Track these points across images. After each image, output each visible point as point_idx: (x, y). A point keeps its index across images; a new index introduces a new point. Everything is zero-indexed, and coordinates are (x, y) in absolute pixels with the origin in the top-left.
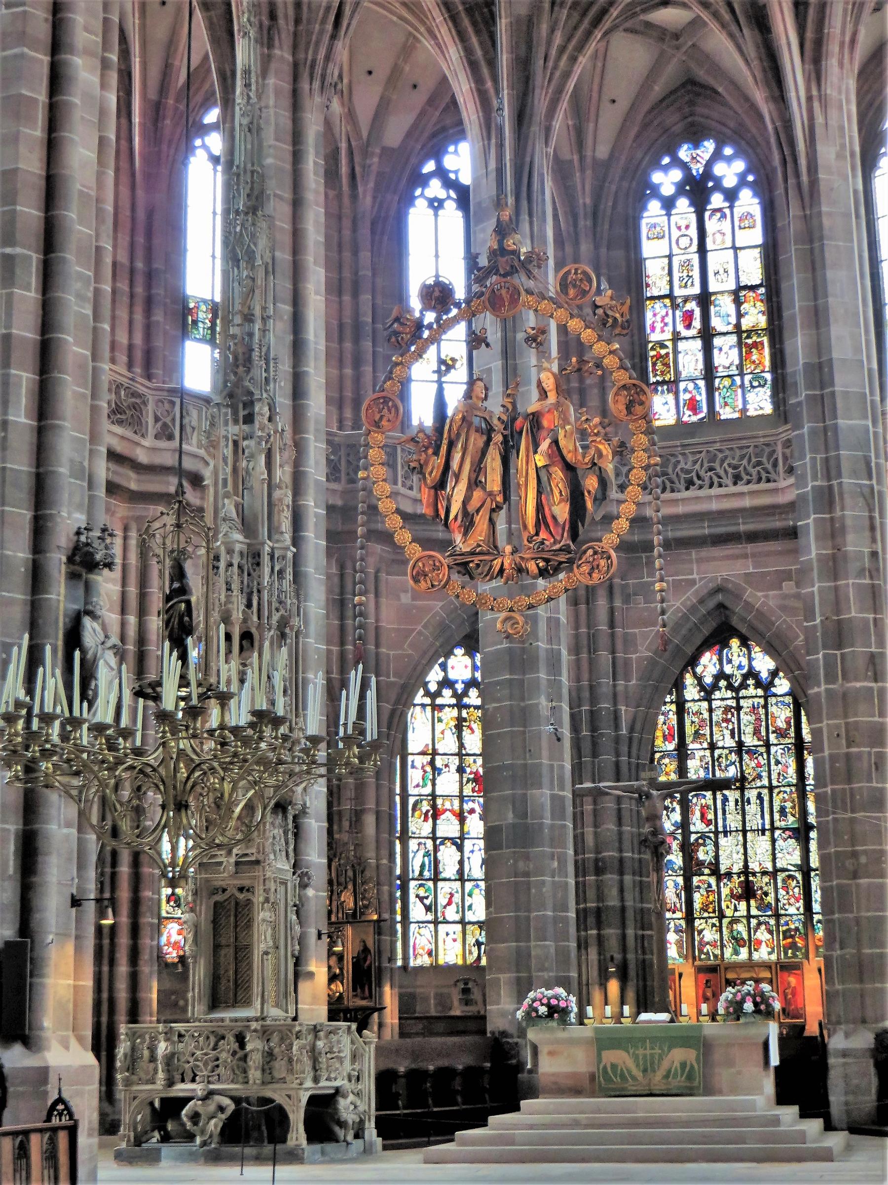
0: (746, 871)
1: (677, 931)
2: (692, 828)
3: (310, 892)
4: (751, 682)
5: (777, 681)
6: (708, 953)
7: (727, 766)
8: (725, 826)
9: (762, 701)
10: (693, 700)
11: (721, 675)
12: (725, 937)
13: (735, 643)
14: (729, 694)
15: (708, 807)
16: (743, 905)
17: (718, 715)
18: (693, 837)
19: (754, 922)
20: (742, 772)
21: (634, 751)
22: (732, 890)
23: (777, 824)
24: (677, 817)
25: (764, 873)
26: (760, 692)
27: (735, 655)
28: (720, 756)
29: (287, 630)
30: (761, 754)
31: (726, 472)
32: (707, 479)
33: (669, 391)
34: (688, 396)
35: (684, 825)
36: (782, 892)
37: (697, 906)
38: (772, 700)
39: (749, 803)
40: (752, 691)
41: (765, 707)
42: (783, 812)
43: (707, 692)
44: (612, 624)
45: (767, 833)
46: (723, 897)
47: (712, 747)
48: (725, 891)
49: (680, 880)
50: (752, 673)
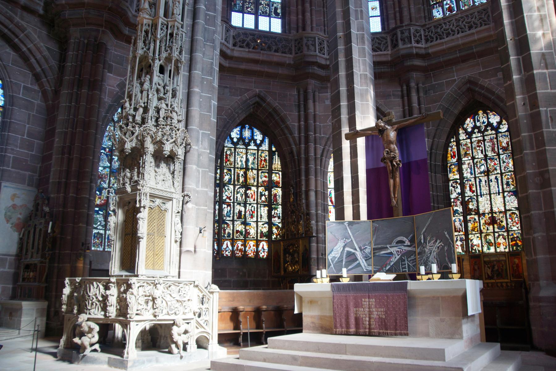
0: (492, 212)
1: (461, 240)
2: (466, 195)
3: (189, 205)
4: (489, 128)
5: (501, 126)
6: (475, 250)
7: (480, 166)
8: (481, 193)
9: (495, 136)
10: (463, 140)
11: (475, 127)
12: (483, 242)
13: (481, 112)
14: (479, 135)
15: (473, 185)
16: (491, 228)
17: (475, 145)
18: (467, 198)
19: (496, 235)
20: (487, 168)
21: (433, 159)
22: (485, 221)
23: (506, 190)
24: (459, 190)
25: (500, 212)
26: (494, 132)
27: (481, 117)
28: (477, 162)
29: (179, 65)
30: (496, 159)
31: (465, 26)
32: (456, 31)
33: (439, 6)
34: (447, 6)
35: (462, 193)
36: (509, 220)
37: (470, 229)
38: (500, 135)
39: (491, 181)
40: (490, 132)
41: (497, 138)
42: (508, 184)
43: (469, 135)
44: (419, 104)
45: (501, 194)
46: (482, 224)
47: (473, 158)
48: (482, 222)
49: (462, 218)
50: (490, 124)
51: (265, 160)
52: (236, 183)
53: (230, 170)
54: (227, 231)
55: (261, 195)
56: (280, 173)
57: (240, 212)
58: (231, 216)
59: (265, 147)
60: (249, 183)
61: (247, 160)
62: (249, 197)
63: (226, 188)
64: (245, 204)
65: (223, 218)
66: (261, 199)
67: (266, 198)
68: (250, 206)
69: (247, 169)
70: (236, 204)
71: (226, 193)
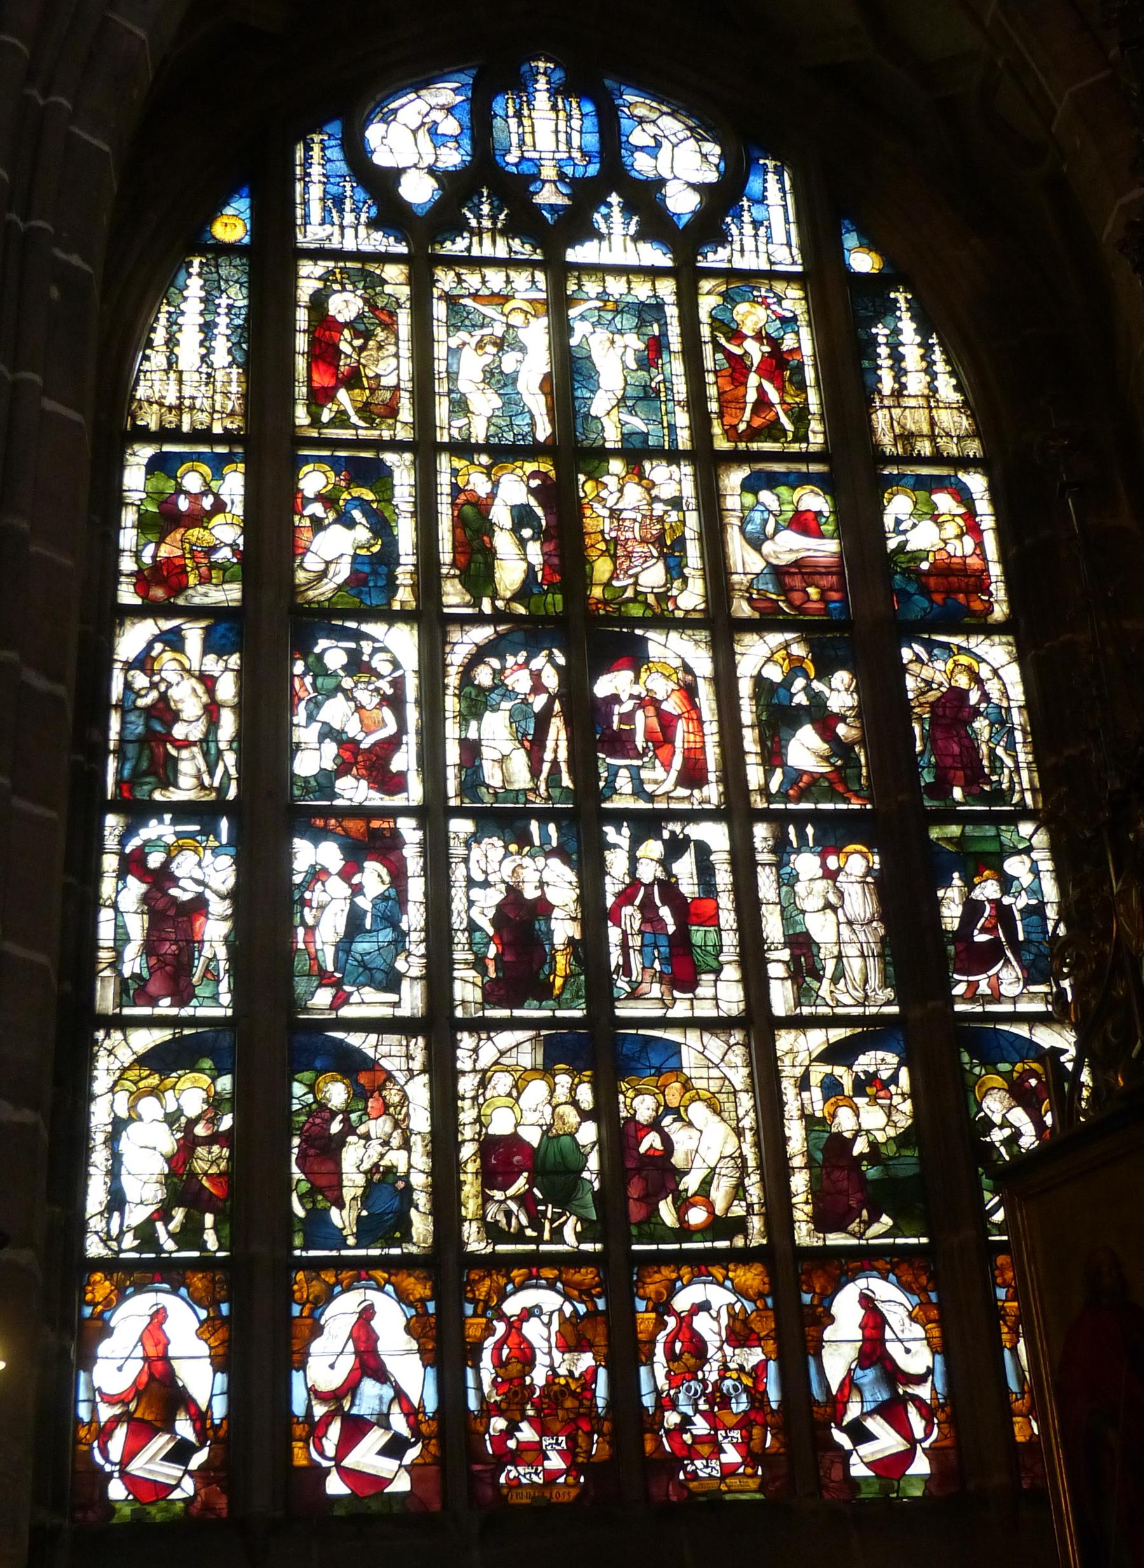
51: (779, 364)
52: (454, 596)
53: (374, 475)
54: (354, 1160)
55: (779, 719)
56: (976, 483)
57: (521, 918)
58: (412, 965)
59: (768, 230)
60: (617, 600)
61: (569, 373)
62: (621, 744)
63: (335, 657)
64: (581, 828)
65: (292, 1004)
66: (773, 757)
67: (840, 748)
68: (653, 849)
69: (571, 453)
70: (461, 827)
71: (336, 711)
